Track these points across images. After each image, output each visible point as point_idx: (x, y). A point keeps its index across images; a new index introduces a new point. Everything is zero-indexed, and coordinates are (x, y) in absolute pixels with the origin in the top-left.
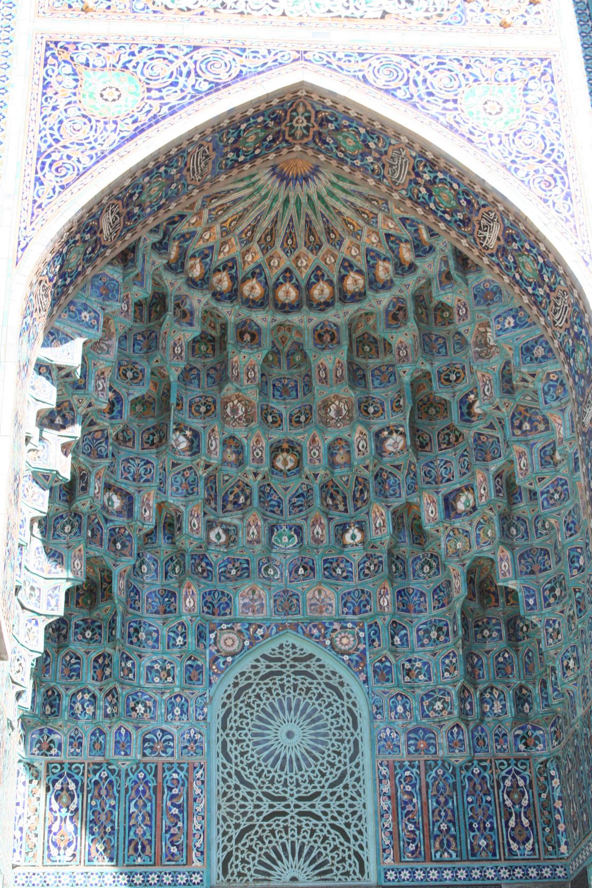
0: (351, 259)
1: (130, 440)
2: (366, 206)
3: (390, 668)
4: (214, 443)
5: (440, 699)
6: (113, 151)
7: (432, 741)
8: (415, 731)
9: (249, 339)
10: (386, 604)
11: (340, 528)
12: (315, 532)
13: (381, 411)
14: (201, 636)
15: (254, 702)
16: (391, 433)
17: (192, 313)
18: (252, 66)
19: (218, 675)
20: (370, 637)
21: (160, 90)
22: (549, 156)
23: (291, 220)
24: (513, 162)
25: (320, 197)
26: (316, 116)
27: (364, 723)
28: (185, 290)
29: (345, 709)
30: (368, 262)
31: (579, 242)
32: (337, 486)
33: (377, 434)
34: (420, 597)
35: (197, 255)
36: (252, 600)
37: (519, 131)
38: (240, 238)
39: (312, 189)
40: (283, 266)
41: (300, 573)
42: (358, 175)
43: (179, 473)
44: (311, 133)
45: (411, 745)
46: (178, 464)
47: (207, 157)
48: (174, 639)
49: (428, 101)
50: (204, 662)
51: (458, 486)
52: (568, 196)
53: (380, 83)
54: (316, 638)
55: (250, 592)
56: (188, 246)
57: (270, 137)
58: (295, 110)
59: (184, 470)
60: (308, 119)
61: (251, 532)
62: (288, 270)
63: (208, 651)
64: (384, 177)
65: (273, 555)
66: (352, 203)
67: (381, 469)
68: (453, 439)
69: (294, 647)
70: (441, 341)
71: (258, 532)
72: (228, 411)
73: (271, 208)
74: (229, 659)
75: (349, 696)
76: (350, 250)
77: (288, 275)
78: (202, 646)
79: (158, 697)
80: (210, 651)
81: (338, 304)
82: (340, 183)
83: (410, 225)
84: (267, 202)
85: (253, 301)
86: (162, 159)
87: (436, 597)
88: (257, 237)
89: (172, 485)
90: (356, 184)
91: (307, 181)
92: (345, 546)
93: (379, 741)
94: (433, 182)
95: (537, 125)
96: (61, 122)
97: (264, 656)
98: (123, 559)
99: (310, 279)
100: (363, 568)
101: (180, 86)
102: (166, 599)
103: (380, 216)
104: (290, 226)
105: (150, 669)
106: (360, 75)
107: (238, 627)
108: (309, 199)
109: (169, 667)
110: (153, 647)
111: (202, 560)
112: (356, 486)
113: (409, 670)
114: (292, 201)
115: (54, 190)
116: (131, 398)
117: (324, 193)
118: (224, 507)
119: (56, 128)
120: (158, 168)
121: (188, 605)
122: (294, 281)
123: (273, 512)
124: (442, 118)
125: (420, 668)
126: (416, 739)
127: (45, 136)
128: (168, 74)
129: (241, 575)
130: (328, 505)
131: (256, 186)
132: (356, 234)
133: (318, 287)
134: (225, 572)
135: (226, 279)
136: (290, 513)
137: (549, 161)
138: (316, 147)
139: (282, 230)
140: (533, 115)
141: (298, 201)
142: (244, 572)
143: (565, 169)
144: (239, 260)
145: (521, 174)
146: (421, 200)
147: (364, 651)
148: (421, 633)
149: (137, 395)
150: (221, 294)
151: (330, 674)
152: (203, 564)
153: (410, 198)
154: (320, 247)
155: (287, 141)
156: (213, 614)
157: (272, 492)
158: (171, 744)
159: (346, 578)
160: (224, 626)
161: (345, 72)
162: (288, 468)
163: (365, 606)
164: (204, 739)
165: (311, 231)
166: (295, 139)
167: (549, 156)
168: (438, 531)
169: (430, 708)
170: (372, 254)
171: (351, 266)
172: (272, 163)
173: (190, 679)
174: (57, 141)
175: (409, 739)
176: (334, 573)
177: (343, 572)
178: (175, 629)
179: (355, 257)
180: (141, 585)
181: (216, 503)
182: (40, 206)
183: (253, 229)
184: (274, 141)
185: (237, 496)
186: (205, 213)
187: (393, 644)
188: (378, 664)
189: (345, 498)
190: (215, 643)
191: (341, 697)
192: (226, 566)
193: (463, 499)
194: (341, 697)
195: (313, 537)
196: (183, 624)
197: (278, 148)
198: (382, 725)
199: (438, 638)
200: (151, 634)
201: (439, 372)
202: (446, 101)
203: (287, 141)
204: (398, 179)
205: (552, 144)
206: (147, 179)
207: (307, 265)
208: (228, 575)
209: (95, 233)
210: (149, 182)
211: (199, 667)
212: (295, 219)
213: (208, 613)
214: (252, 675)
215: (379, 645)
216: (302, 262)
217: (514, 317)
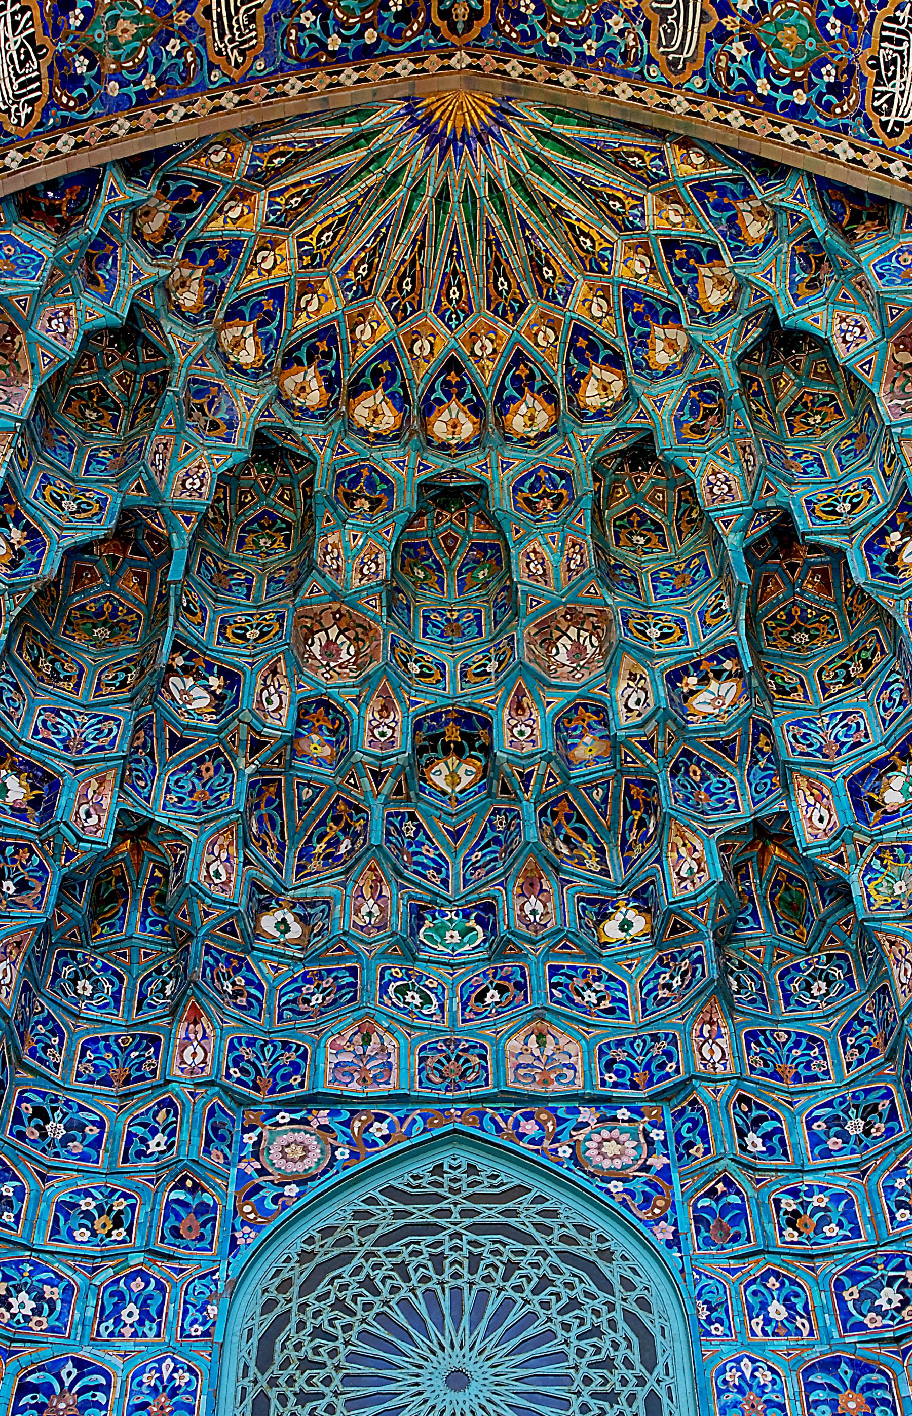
1: (68, 678)
3: (741, 1207)
4: (275, 699)
5: (890, 1282)
7: (879, 1394)
8: (830, 1365)
9: (367, 506)
10: (718, 1056)
11: (593, 909)
12: (528, 908)
13: (678, 633)
14: (216, 1135)
15: (354, 1299)
16: (704, 680)
17: (231, 425)
19: (256, 1227)
20: (679, 1137)
23: (455, 240)
27: (673, 1347)
29: (618, 1315)
30: (630, 331)
32: (580, 819)
33: (674, 677)
34: (809, 1047)
36: (360, 1057)
39: (494, 162)
41: (488, 1000)
43: (188, 768)
45: (817, 1403)
46: (186, 742)
48: (144, 1141)
50: (222, 1194)
51: (882, 752)
54: (532, 1141)
55: (358, 1038)
59: (200, 760)
61: (364, 910)
62: (452, 365)
63: (234, 1172)
64: (651, 60)
65: (419, 967)
66: (584, 177)
67: (685, 753)
68: (855, 670)
69: (472, 1169)
71: (382, 910)
72: (316, 649)
74: (291, 1190)
75: (628, 1285)
76: (587, 306)
77: (453, 378)
78: (216, 1159)
79: (78, 1279)
80: (242, 1174)
83: (716, 207)
84: (400, 193)
85: (377, 436)
87: (850, 1041)
89: (168, 790)
90: (592, 124)
92: (604, 945)
93: (720, 1392)
97: (390, 1191)
98: (16, 912)
99: (502, 388)
100: (655, 989)
102: (134, 1054)
105: (66, 1208)
107: (323, 1117)
109: (120, 1205)
110: (84, 1157)
111: (236, 971)
112: (627, 815)
113: (795, 1213)
114: (456, 194)
116: (67, 543)
118: (301, 868)
121: (189, 1060)
123: (425, 877)
125: (826, 1209)
126: (832, 1388)
129: (335, 1001)
130: (557, 852)
132: (594, 263)
133: (523, 409)
134: (294, 1001)
135: (314, 384)
136: (466, 882)
141: (469, 197)
142: (348, 992)
146: (739, 80)
147: (665, 1172)
148: (819, 1127)
149: (81, 537)
151: (573, 1232)
152: (240, 981)
153: (712, 92)
154: (522, 308)
156: (257, 1088)
157: (421, 837)
158: (101, 1397)
159: (610, 1011)
160: (284, 1117)
162: (458, 789)
163: (662, 1066)
164: (200, 1385)
165: (497, 266)
166: (452, 27)
168: (839, 859)
169: (866, 1306)
171: (593, 347)
172: (406, 92)
173: (175, 1232)
175: (811, 1387)
176: (577, 999)
177: (600, 999)
178: (149, 1119)
180: (71, 1022)
181: (281, 857)
185: (335, 843)
187: (743, 1148)
188: (706, 1202)
189: (601, 851)
190: (256, 1155)
191: (607, 1287)
192: (299, 989)
193: (898, 782)
194: (605, 1285)
195: (523, 918)
196: (168, 1104)
197: (416, 47)
198: (728, 1351)
199: (867, 1133)
200: (81, 1127)
201: (808, 502)
203: (436, 31)
204: (680, 50)
207: (495, 351)
208: (303, 1007)
211: (203, 1208)
212: (464, 239)
213: (239, 1081)
214: (353, 1233)
215: (707, 1151)
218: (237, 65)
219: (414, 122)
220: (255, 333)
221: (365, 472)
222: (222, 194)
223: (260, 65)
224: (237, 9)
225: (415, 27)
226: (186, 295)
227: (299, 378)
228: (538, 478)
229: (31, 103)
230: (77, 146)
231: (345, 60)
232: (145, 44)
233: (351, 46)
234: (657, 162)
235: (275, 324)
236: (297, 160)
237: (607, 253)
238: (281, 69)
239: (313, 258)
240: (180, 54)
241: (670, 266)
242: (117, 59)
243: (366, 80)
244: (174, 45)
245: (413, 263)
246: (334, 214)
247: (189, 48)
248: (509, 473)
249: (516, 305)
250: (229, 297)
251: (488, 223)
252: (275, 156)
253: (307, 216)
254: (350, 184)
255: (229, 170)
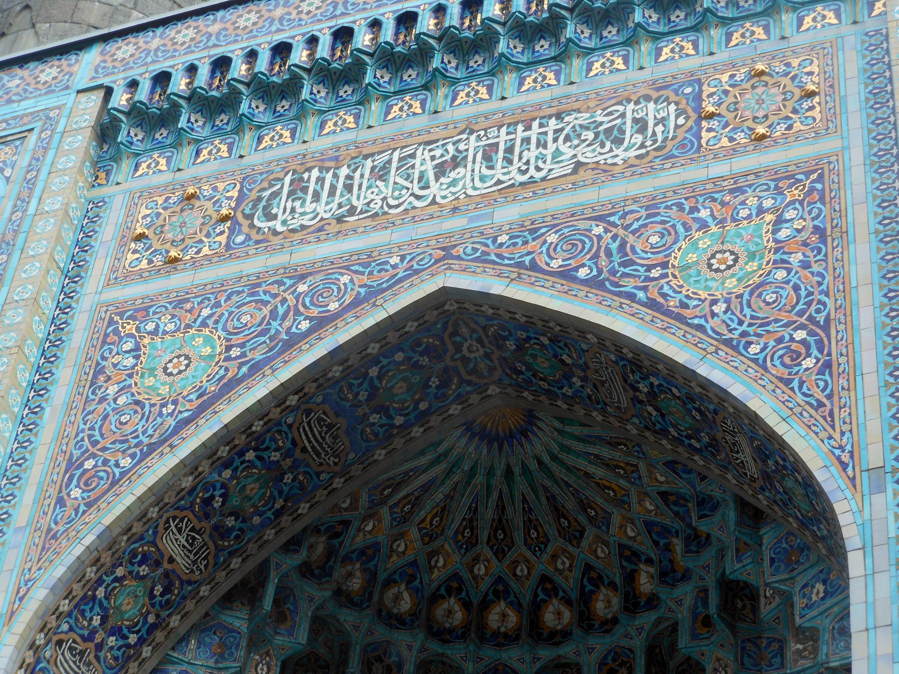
0: (630, 543)
2: (616, 455)
6: (165, 440)
18: (374, 284)
21: (242, 345)
22: (801, 314)
23: (525, 500)
24: (744, 334)
25: (554, 458)
26: (487, 336)
28: (381, 632)
30: (656, 543)
31: (837, 436)
35: (397, 577)
37: (759, 286)
38: (457, 542)
40: (536, 574)
42: (580, 411)
44: (496, 362)
47: (330, 426)
49: (625, 275)
52: (828, 365)
53: (555, 264)
56: (376, 566)
57: (434, 382)
58: (455, 333)
60: (479, 340)
66: (597, 456)
70: (775, 646)
73: (489, 488)
81: (624, 618)
82: (568, 429)
84: (479, 479)
85: (506, 635)
86: (240, 440)
88: (484, 535)
91: (526, 437)
94: (653, 394)
95: (789, 271)
96: (106, 417)
99: (583, 587)
101: (273, 332)
103: (642, 466)
104: (528, 510)
106: (527, 259)
108: (540, 462)
114: (517, 471)
115: (77, 510)
117: (556, 449)
119: (97, 426)
120: (241, 454)
122: (561, 594)
124: (641, 295)
127: (82, 440)
128: (259, 319)
131: (452, 458)
132: (621, 502)
133: (601, 597)
135: (457, 608)
137: (803, 320)
138: (513, 382)
139: (517, 519)
140: (785, 257)
141: (525, 470)
143: (826, 327)
144: (465, 575)
145: (754, 349)
150: (451, 631)
155: (469, 383)
161: (506, 262)
165: (559, 512)
167: (801, 314)
170: (656, 529)
174: (94, 443)
179: (633, 539)
182: (54, 537)
183: (471, 523)
184: (444, 384)
186: (385, 511)
197: (459, 396)
202: (649, 268)
203: (469, 383)
205: (810, 294)
206: (227, 473)
207: (571, 565)
209: (158, 564)
210: (232, 477)
212: (531, 497)
216: (563, 563)
217: (824, 582)
218: (335, 464)
219: (473, 436)
220: (407, 588)
221: (500, 667)
222: (356, 524)
223: (351, 456)
224: (324, 439)
225: (454, 387)
226: (355, 580)
227: (445, 605)
228: (616, 653)
229: (205, 558)
230: (244, 560)
231: (413, 425)
232: (269, 487)
233: (412, 416)
234: (636, 448)
235: (418, 580)
236: (397, 487)
237: (626, 498)
238: (368, 451)
239: (431, 537)
240: (294, 480)
241: (668, 505)
242: (253, 506)
243: (430, 428)
244: (288, 478)
245: (500, 520)
246: (437, 505)
247: (299, 474)
248: (594, 655)
249: (577, 534)
250: (382, 576)
251: (544, 487)
252: (384, 490)
253: (420, 510)
254: (442, 483)
255: (356, 509)
